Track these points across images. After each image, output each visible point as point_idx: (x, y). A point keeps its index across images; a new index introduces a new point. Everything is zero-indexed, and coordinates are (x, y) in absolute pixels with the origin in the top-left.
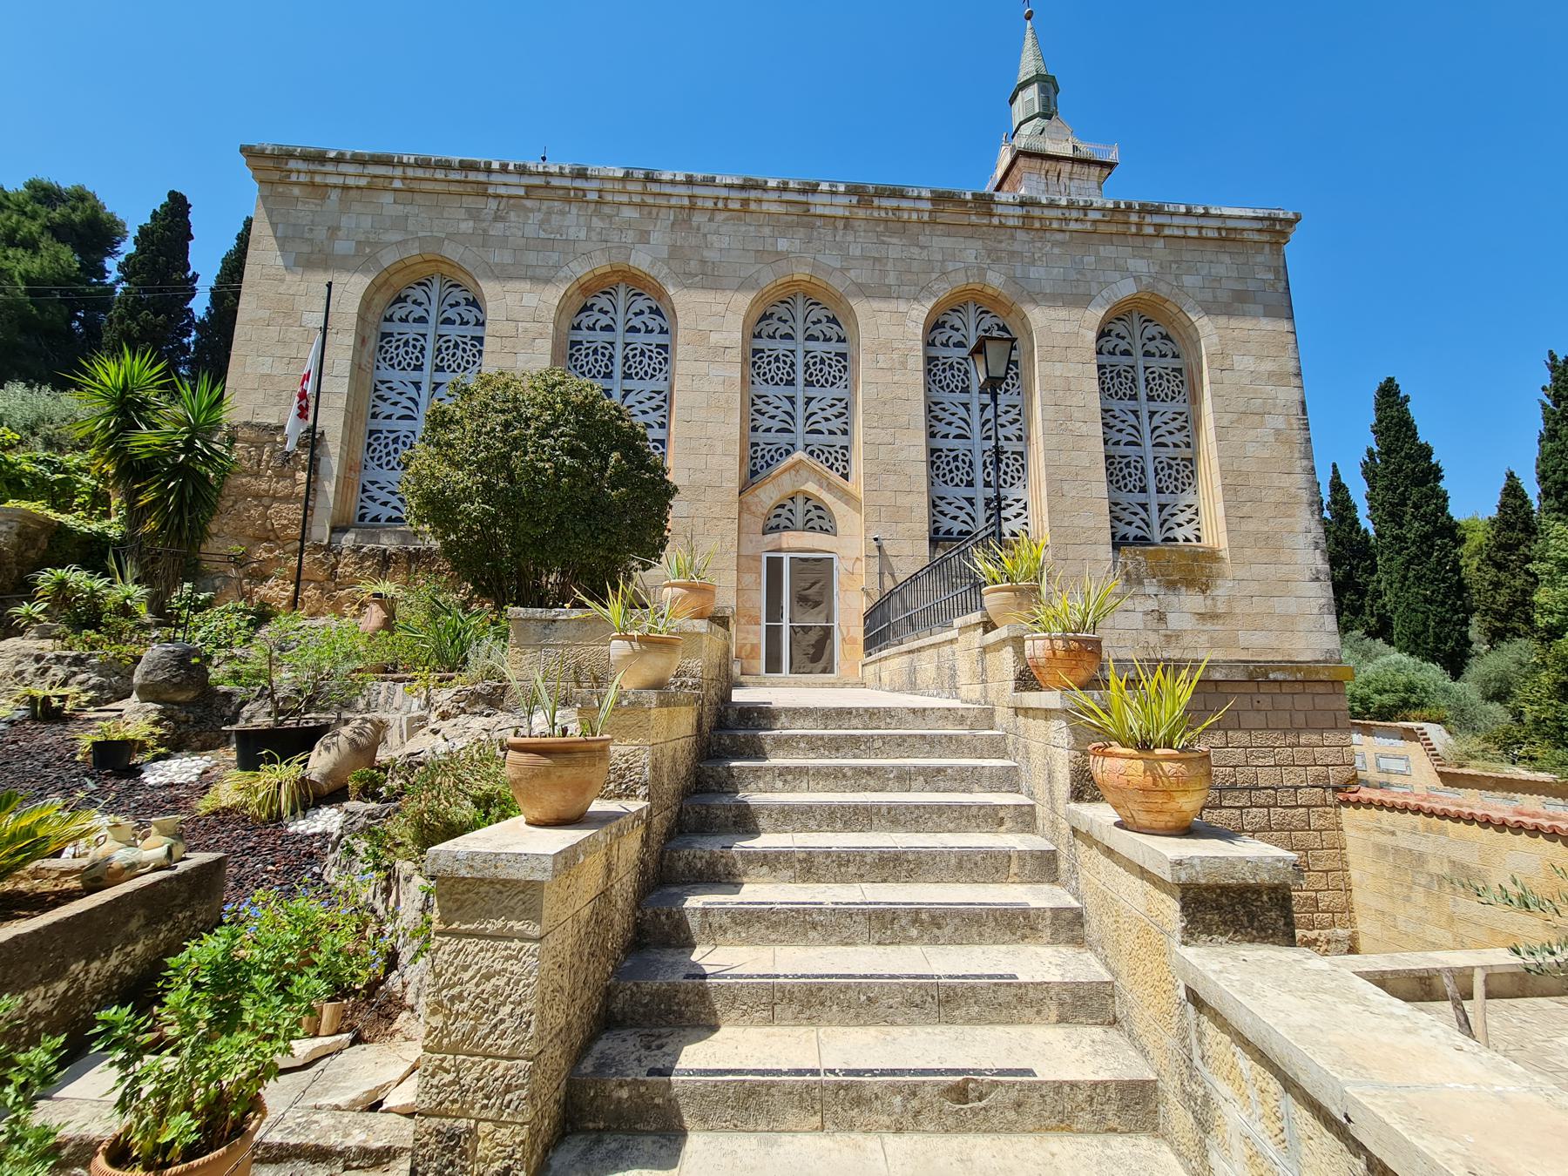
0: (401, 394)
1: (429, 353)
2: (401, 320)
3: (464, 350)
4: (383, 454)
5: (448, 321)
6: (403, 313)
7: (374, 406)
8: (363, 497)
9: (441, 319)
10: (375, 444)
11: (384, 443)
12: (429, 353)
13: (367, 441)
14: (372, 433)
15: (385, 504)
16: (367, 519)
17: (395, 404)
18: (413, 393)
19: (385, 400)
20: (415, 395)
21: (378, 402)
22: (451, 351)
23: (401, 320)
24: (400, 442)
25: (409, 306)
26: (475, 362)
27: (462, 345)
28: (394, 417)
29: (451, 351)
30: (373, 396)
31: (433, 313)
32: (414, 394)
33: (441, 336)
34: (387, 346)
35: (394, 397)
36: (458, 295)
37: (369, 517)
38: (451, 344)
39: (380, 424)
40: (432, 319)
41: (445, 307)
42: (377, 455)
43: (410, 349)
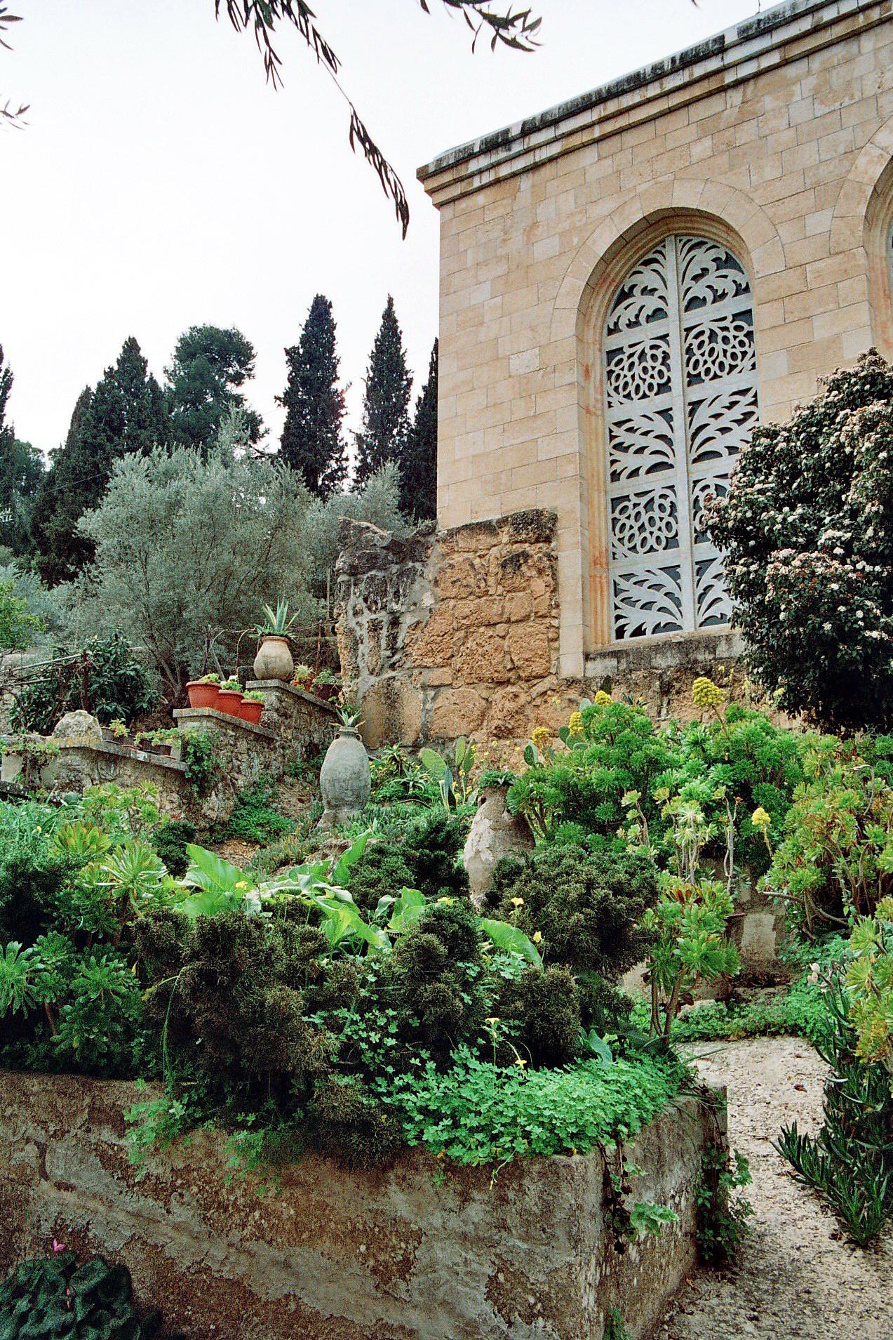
0: (646, 433)
1: (676, 360)
2: (630, 325)
3: (725, 340)
4: (635, 531)
5: (695, 303)
6: (630, 315)
7: (613, 462)
8: (617, 601)
9: (685, 303)
10: (623, 519)
11: (633, 513)
12: (676, 360)
13: (611, 516)
14: (615, 501)
15: (647, 606)
16: (627, 634)
17: (640, 451)
18: (660, 426)
19: (626, 449)
20: (666, 431)
21: (618, 455)
22: (706, 348)
23: (630, 325)
24: (656, 506)
25: (638, 299)
26: (744, 354)
27: (721, 334)
28: (642, 472)
29: (706, 348)
30: (609, 448)
31: (672, 297)
32: (665, 430)
33: (688, 330)
34: (617, 370)
35: (637, 440)
36: (703, 258)
37: (629, 630)
38: (705, 338)
39: (626, 487)
40: (672, 309)
41: (688, 282)
42: (627, 534)
43: (649, 364)
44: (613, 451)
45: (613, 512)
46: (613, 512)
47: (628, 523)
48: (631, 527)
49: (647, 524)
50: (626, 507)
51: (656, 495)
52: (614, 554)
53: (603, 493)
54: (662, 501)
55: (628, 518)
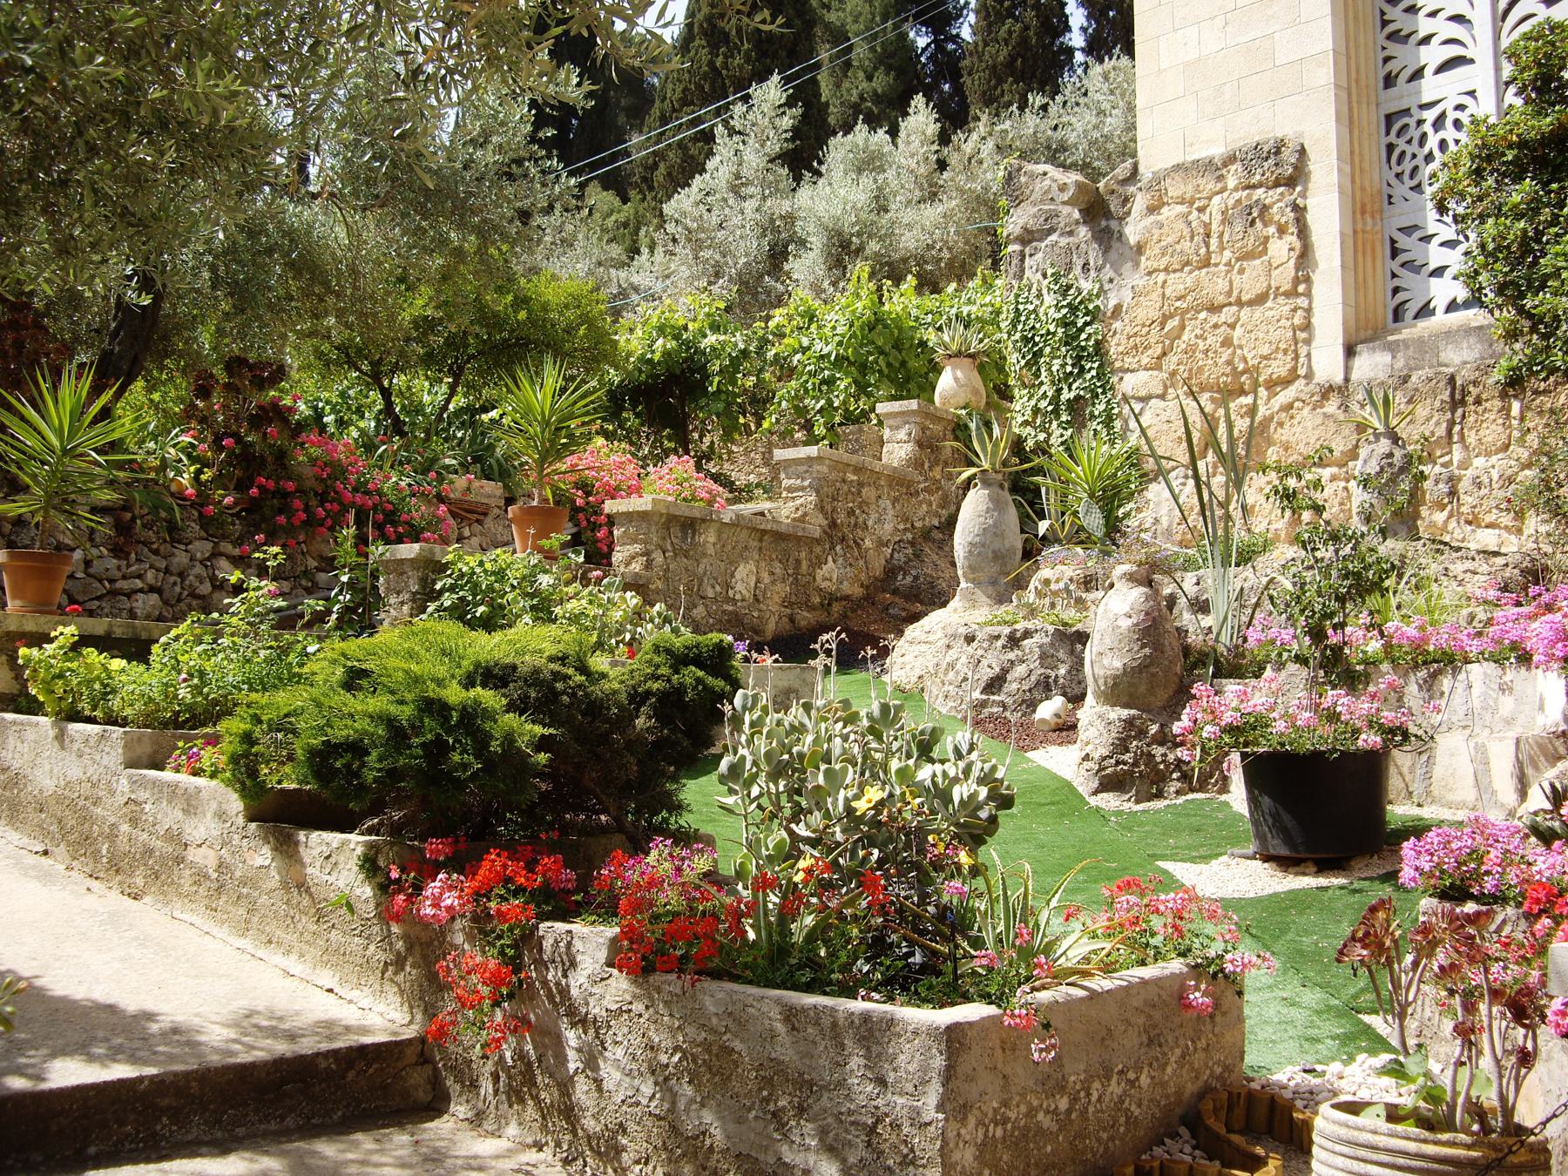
0: (1433, 14)
4: (1420, 160)
7: (1387, 60)
8: (1395, 265)
10: (1401, 144)
11: (1416, 135)
13: (1385, 141)
14: (1390, 119)
21: (1394, 49)
37: (1413, 308)
42: (1407, 166)
44: (1387, 44)
45: (1388, 133)
46: (1388, 133)
47: (1409, 150)
48: (1414, 156)
49: (1436, 152)
50: (1406, 126)
51: (1448, 105)
52: (1390, 197)
53: (1373, 107)
54: (1458, 114)
55: (1409, 142)
